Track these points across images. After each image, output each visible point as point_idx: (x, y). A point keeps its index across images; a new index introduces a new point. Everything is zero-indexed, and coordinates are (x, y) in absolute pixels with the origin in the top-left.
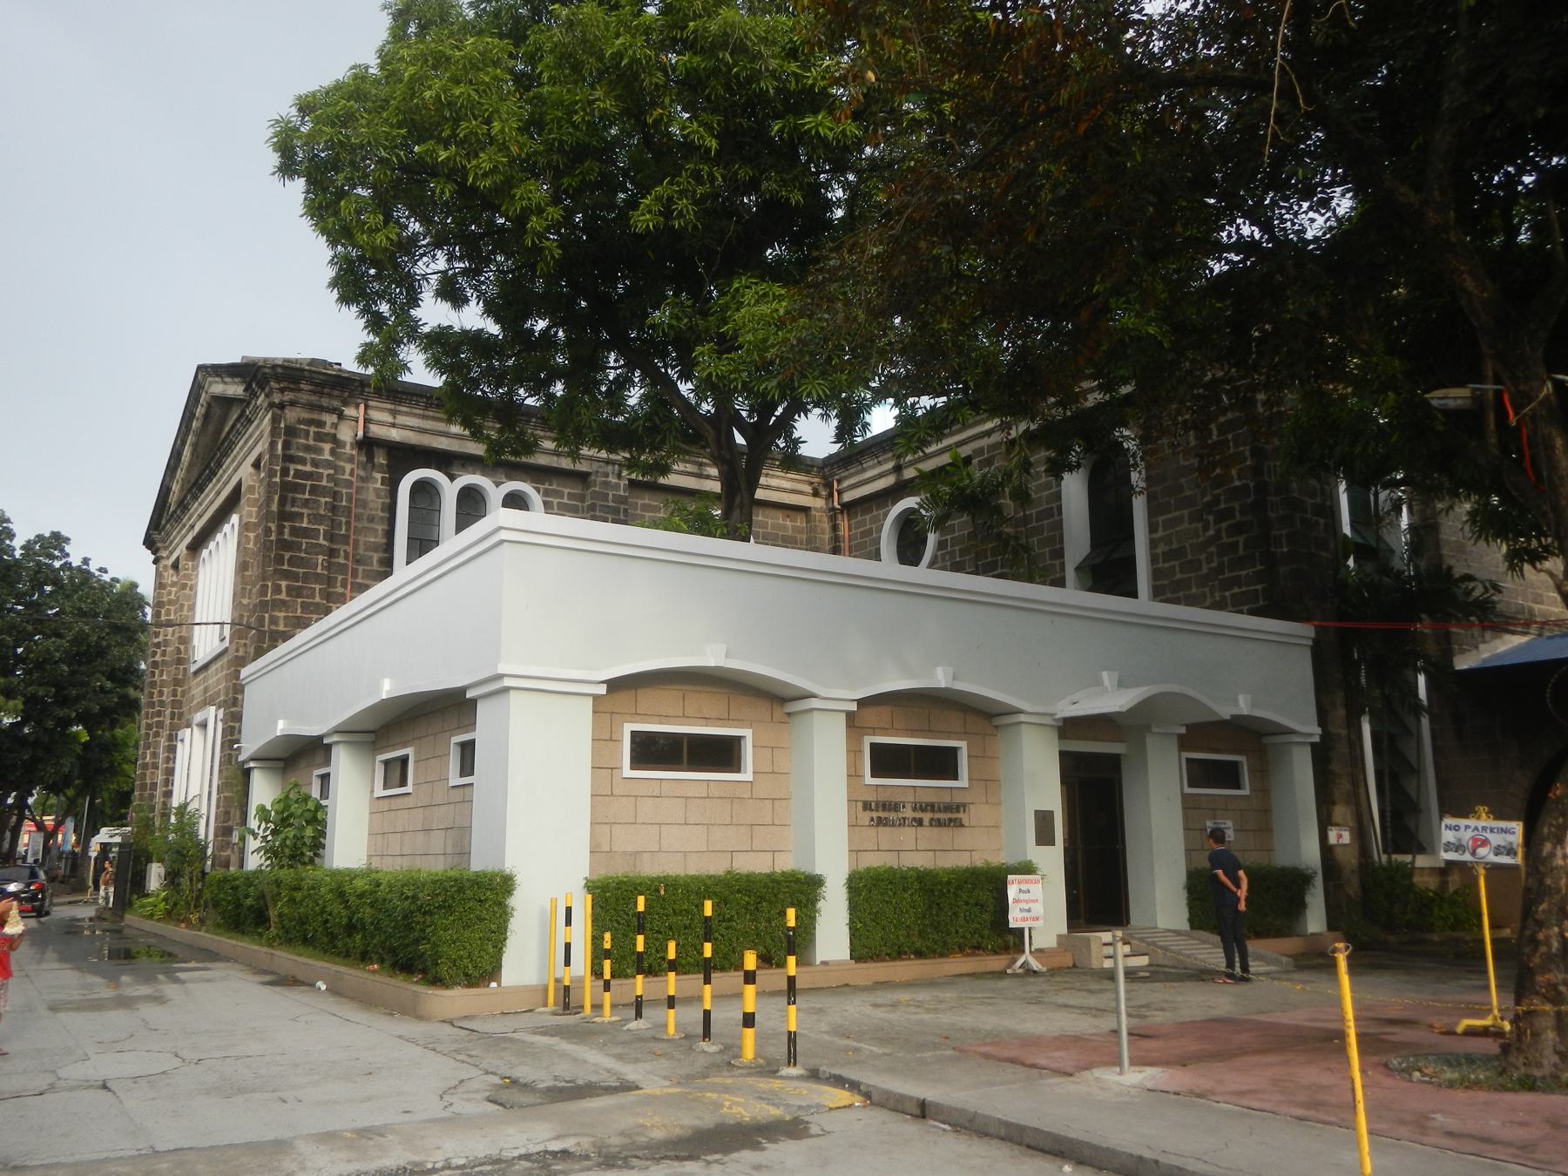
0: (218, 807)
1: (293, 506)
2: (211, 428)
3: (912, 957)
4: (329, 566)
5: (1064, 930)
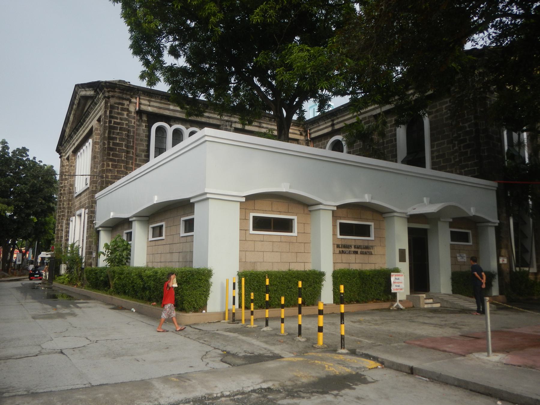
0: (87, 244)
1: (113, 135)
2: (80, 108)
3: (355, 302)
4: (127, 157)
5: (408, 293)
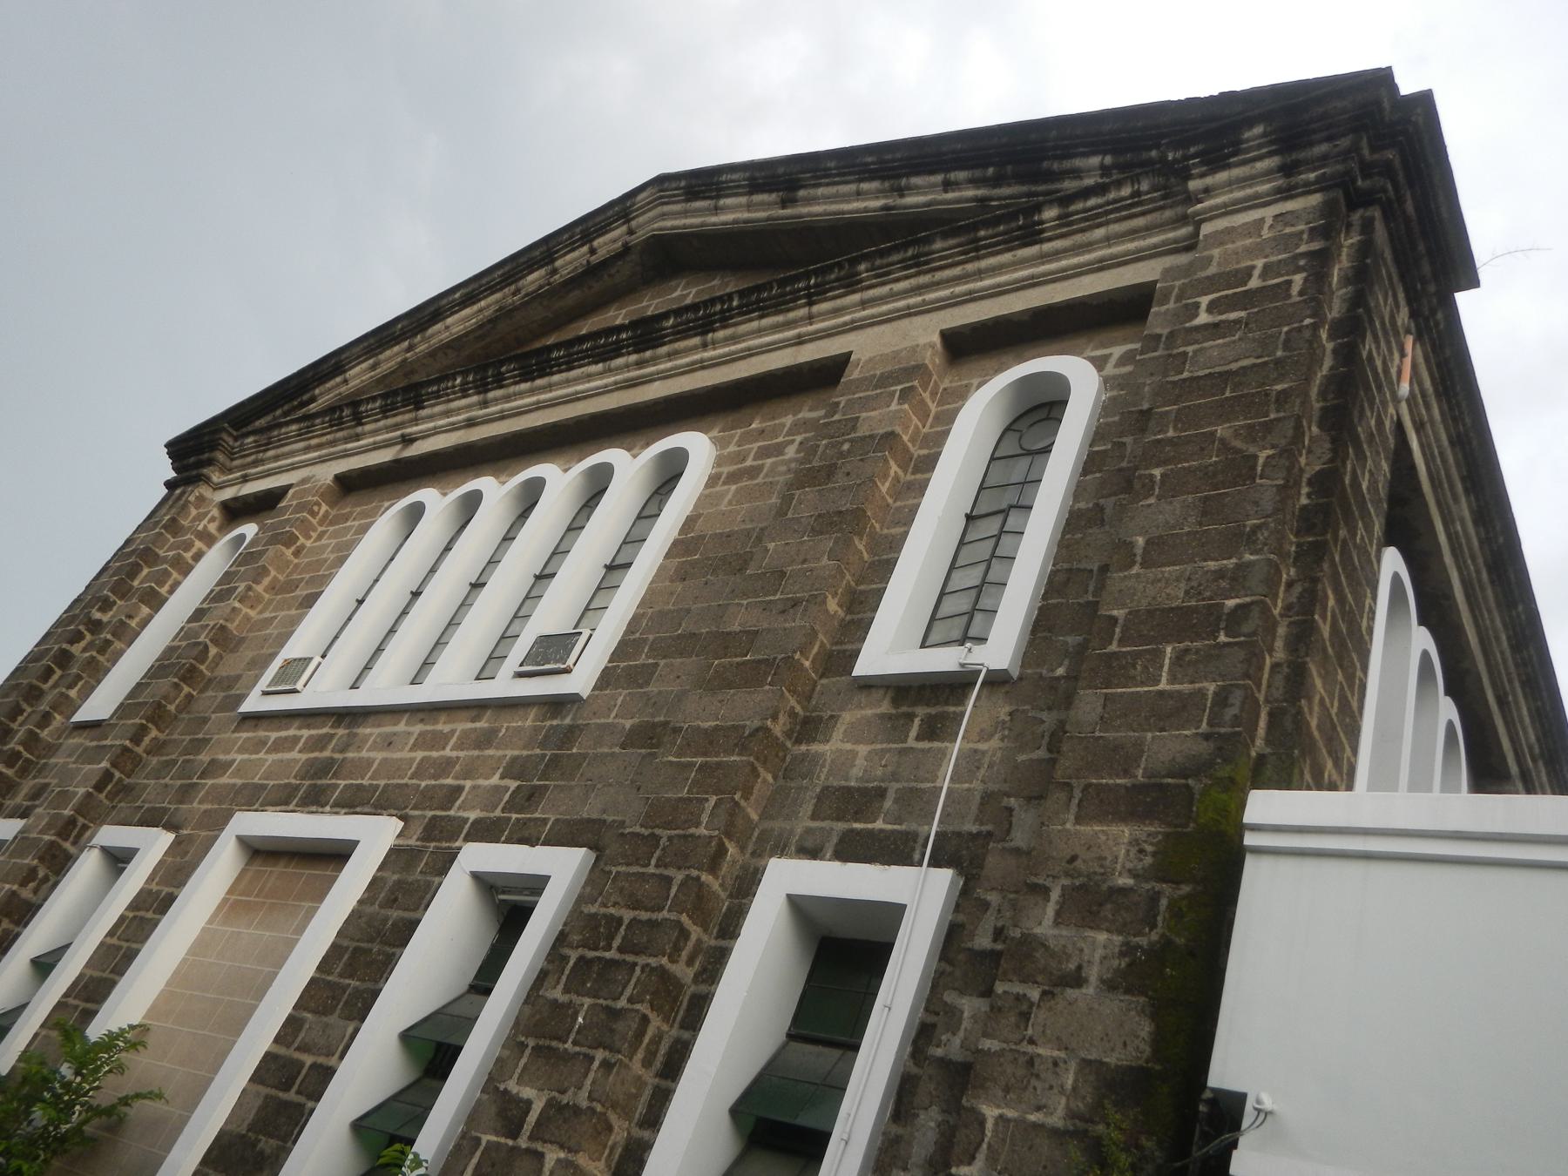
2: (574, 297)
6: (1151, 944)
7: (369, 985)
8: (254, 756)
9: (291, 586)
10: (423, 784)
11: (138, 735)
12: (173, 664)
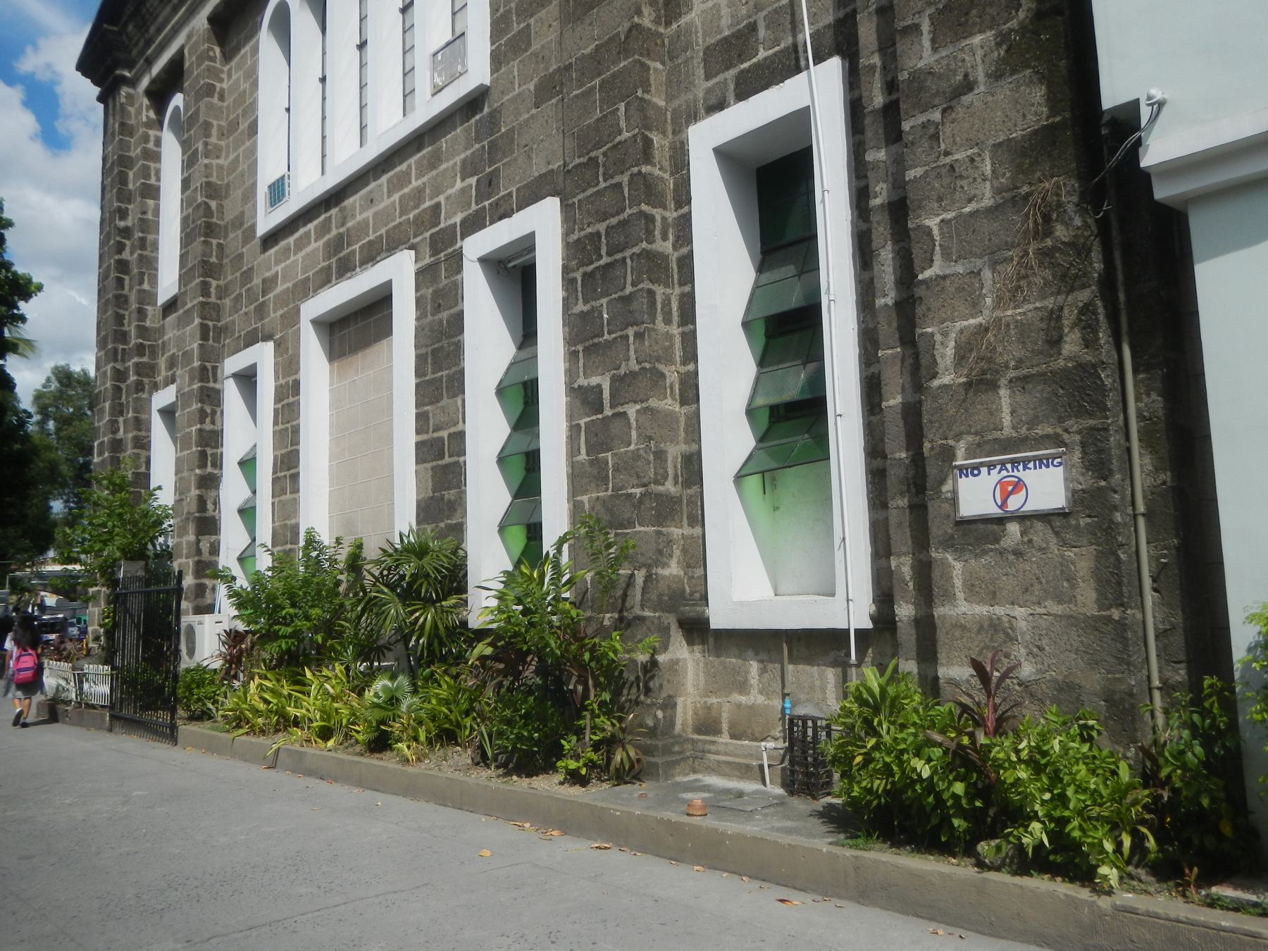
0: (573, 451)
6: (1021, 24)
7: (454, 369)
8: (288, 262)
9: (234, 125)
10: (411, 216)
11: (205, 289)
12: (193, 229)
